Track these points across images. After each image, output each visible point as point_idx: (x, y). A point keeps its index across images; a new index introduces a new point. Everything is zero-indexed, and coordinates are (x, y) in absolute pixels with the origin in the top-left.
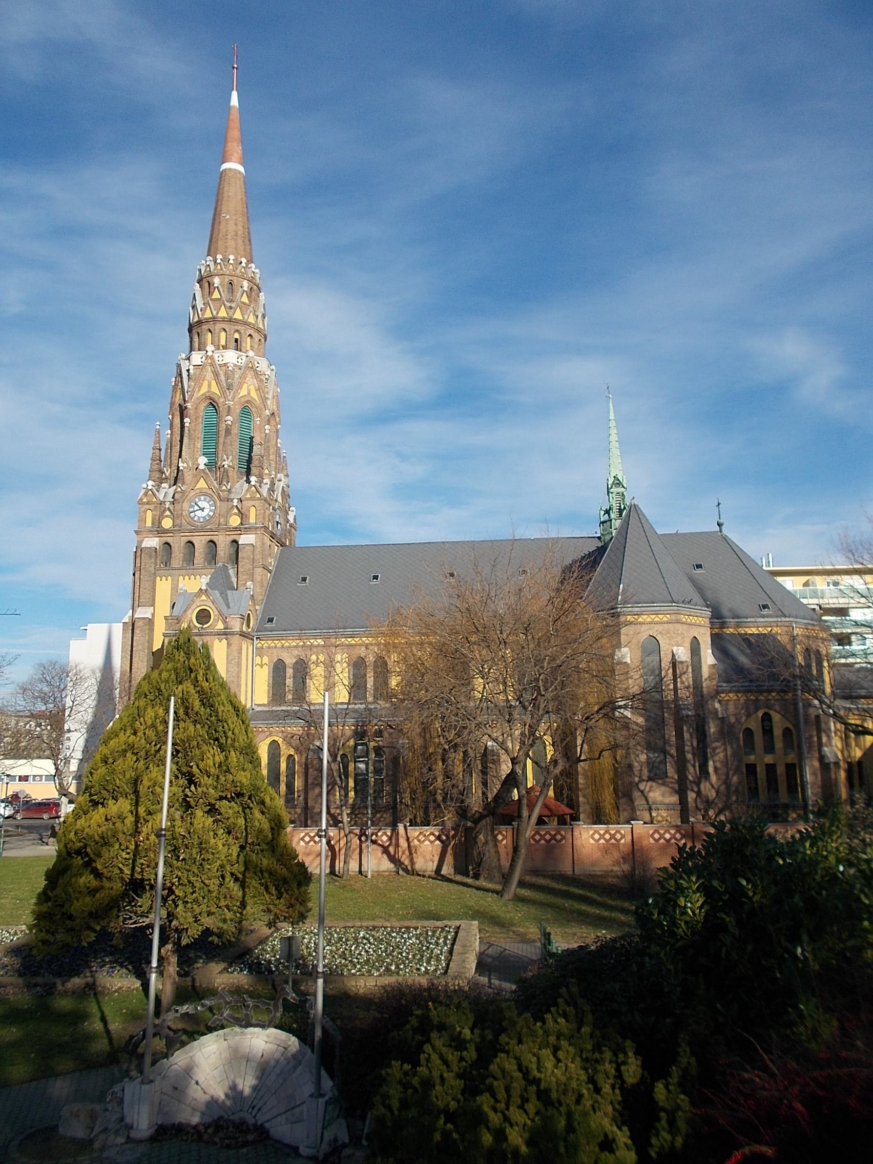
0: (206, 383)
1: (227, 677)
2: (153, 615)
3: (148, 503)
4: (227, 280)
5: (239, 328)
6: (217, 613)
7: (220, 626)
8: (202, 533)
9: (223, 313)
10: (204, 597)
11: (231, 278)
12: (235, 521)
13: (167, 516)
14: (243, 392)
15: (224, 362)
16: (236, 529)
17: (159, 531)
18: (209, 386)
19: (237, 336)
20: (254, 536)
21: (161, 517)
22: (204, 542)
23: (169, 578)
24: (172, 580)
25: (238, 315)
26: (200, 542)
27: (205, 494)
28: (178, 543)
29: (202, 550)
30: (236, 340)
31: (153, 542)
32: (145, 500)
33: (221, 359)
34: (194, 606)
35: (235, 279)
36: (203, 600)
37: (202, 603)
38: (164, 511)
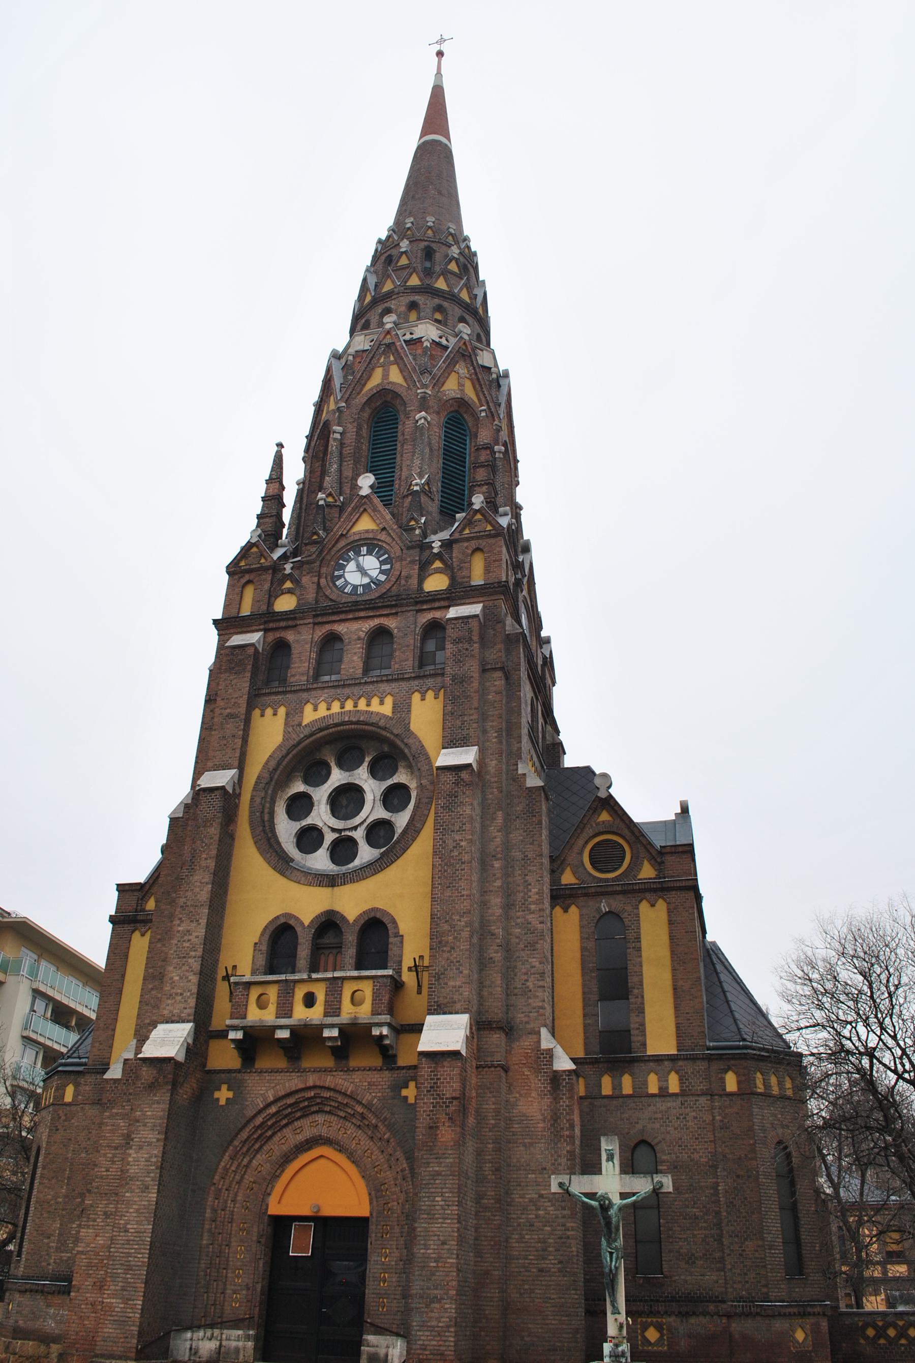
0: (378, 373)
4: (423, 245)
5: (446, 304)
9: (414, 281)
18: (386, 375)
23: (282, 711)
25: (441, 284)
35: (434, 246)
38: (283, 582)
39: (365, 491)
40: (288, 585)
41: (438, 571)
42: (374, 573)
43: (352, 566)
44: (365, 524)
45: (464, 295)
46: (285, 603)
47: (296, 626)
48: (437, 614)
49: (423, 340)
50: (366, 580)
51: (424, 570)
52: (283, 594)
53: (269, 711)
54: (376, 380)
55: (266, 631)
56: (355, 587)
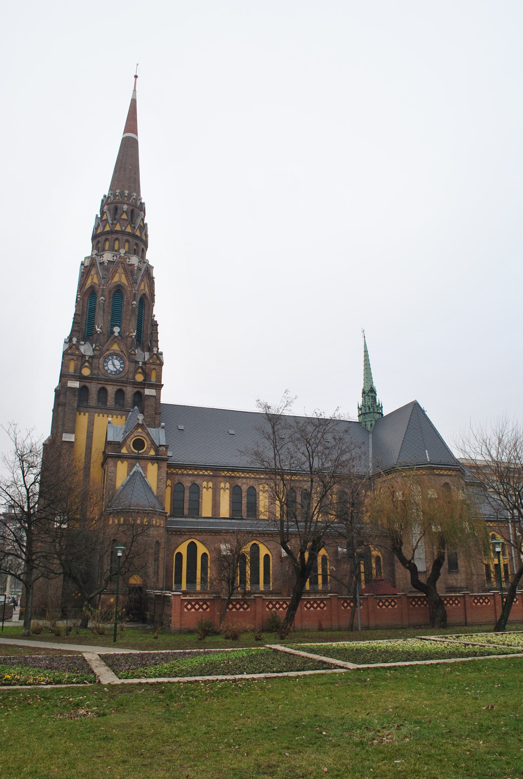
0: (117, 275)
1: (157, 492)
2: (76, 439)
3: (72, 354)
4: (131, 208)
6: (149, 443)
7: (152, 453)
8: (114, 383)
9: (129, 230)
10: (140, 430)
11: (133, 208)
12: (140, 378)
13: (86, 367)
14: (142, 287)
15: (130, 263)
16: (140, 384)
17: (80, 378)
18: (120, 277)
19: (135, 248)
20: (155, 390)
21: (82, 366)
22: (115, 390)
24: (89, 415)
25: (138, 233)
26: (111, 390)
27: (117, 355)
28: (94, 388)
29: (113, 396)
30: (135, 250)
31: (76, 384)
32: (69, 352)
33: (128, 260)
34: (133, 436)
36: (140, 432)
37: (138, 434)
39: (116, 334)
40: (87, 364)
41: (140, 373)
42: (118, 367)
43: (110, 362)
44: (115, 347)
45: (144, 238)
46: (86, 372)
47: (91, 382)
48: (140, 390)
49: (135, 265)
50: (115, 370)
51: (135, 372)
52: (84, 367)
53: (82, 414)
54: (116, 279)
55: (80, 381)
56: (112, 371)
